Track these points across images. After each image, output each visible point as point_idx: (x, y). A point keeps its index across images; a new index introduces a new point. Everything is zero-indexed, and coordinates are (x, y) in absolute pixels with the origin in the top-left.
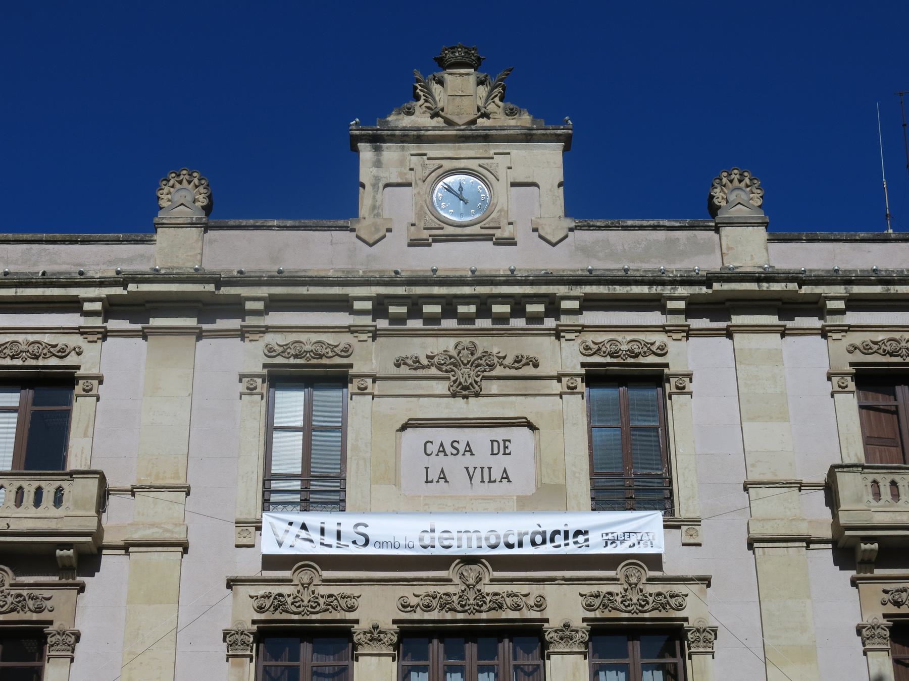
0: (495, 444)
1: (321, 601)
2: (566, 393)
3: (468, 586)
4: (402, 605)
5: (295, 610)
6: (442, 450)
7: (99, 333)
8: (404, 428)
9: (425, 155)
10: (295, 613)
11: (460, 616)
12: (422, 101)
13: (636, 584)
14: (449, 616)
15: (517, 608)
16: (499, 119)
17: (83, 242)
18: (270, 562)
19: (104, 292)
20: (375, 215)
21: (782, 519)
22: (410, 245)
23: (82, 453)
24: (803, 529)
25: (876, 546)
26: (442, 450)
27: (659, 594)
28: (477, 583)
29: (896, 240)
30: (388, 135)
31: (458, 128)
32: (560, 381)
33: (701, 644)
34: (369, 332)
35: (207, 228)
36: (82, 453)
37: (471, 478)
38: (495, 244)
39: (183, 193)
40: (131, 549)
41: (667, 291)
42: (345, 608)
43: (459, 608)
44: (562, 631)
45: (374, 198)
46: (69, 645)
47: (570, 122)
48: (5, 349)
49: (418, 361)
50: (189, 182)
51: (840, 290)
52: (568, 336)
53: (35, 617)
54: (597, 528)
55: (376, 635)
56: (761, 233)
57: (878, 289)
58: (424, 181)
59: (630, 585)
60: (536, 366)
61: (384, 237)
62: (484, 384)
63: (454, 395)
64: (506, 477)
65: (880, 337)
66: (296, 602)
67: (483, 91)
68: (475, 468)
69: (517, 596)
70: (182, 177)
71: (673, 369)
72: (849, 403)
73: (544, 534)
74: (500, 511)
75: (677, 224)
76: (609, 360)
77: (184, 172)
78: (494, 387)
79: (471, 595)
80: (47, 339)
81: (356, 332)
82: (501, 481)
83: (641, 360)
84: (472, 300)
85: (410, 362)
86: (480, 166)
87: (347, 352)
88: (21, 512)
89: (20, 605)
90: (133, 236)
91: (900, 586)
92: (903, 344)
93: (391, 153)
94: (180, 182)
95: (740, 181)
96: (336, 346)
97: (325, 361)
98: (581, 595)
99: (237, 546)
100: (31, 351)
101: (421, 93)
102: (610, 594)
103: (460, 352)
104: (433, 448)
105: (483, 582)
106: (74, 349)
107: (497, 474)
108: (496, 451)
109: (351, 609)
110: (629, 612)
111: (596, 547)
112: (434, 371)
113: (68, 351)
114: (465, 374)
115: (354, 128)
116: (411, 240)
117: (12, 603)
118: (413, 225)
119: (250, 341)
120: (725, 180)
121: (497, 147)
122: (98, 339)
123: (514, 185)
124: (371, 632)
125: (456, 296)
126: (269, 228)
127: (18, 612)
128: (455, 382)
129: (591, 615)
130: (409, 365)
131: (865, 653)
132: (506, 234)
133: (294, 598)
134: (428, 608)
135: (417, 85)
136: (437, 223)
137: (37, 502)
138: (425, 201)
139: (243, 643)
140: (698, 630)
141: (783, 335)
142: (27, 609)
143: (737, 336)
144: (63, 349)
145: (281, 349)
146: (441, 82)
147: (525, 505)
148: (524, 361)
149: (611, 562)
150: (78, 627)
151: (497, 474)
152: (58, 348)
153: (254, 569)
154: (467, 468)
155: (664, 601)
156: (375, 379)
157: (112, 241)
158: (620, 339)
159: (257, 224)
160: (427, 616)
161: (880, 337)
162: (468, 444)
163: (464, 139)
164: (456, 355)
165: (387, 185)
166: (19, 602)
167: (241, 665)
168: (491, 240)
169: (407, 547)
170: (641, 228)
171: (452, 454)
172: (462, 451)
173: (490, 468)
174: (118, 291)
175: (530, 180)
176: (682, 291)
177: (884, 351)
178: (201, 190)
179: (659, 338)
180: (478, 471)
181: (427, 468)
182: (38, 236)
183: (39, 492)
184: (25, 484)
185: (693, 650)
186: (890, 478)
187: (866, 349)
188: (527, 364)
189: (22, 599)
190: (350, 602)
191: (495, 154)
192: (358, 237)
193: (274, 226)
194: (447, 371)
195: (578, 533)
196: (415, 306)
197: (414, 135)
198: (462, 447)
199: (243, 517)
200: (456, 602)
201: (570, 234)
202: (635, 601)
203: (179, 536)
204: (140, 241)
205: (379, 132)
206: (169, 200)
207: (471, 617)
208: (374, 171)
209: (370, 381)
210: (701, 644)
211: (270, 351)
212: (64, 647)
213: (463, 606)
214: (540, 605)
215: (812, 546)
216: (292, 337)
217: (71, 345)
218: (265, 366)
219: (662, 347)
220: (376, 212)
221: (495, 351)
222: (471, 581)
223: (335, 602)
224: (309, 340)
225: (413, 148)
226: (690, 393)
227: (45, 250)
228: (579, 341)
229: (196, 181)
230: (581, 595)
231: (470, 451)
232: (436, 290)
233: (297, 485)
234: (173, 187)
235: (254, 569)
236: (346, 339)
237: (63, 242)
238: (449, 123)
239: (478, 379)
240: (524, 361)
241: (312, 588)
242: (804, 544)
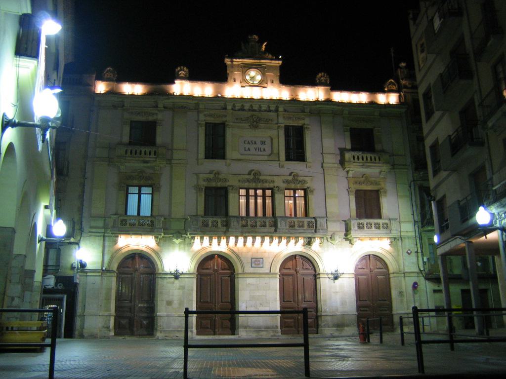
64: (264, 149)
104: (246, 142)
107: (262, 150)
184: (147, 150)
198: (253, 142)
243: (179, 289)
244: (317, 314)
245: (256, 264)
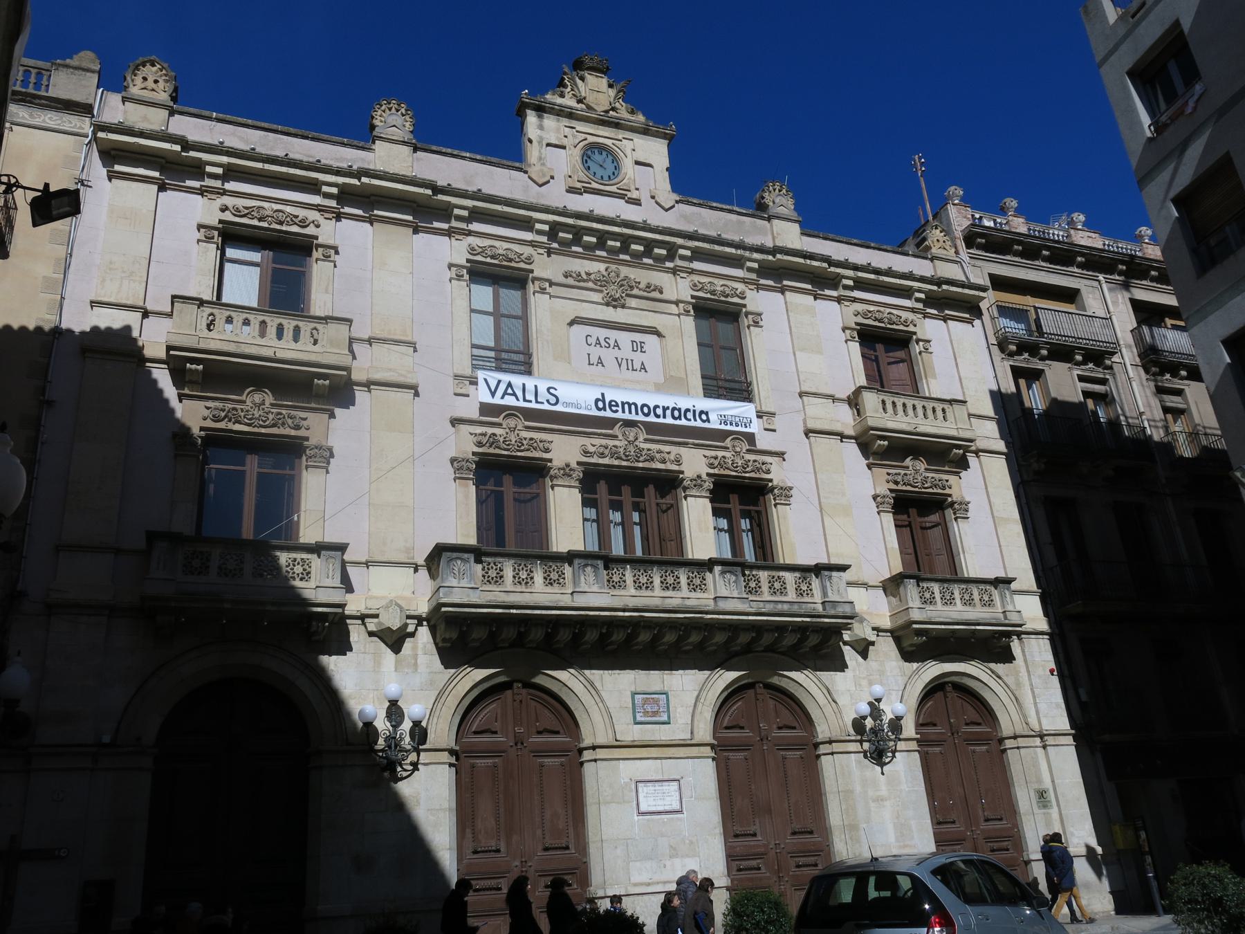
0: (635, 344)
1: (525, 442)
2: (683, 314)
3: (629, 442)
4: (583, 450)
5: (506, 447)
6: (598, 343)
7: (334, 212)
8: (571, 323)
9: (574, 128)
10: (505, 450)
11: (624, 463)
12: (569, 89)
13: (740, 452)
14: (616, 463)
15: (664, 462)
16: (623, 113)
17: (313, 139)
18: (486, 409)
19: (341, 180)
20: (541, 164)
21: (826, 419)
22: (568, 191)
23: (325, 305)
24: (837, 427)
25: (886, 443)
26: (598, 343)
27: (755, 461)
28: (635, 440)
29: (874, 248)
30: (549, 108)
31: (599, 113)
32: (677, 306)
33: (783, 498)
34: (545, 248)
35: (416, 149)
36: (325, 305)
37: (620, 366)
38: (627, 202)
39: (394, 117)
40: (372, 387)
41: (747, 254)
42: (543, 449)
43: (624, 458)
44: (695, 480)
45: (540, 151)
46: (325, 458)
47: (673, 126)
48: (252, 211)
49: (580, 276)
50: (398, 111)
51: (850, 273)
52: (682, 275)
53: (293, 433)
54: (714, 410)
55: (567, 470)
56: (796, 228)
57: (872, 276)
58: (575, 147)
59: (736, 452)
60: (661, 292)
61: (548, 182)
62: (628, 299)
63: (607, 304)
64: (643, 368)
65: (872, 308)
66: (506, 441)
67: (612, 92)
68: (622, 359)
69: (663, 452)
70: (392, 105)
71: (750, 308)
72: (855, 347)
73: (679, 410)
74: (646, 391)
75: (744, 212)
76: (709, 296)
77: (394, 102)
78: (633, 302)
79: (632, 449)
80: (289, 209)
81: (536, 246)
82: (640, 371)
83: (730, 299)
84: (619, 238)
85: (574, 275)
86: (613, 144)
87: (529, 260)
88: (282, 344)
89: (280, 422)
90: (355, 142)
91: (897, 471)
92: (886, 315)
93: (550, 121)
94: (390, 109)
95: (780, 191)
96: (522, 255)
97: (513, 264)
98: (705, 457)
99: (456, 394)
100: (275, 217)
101: (569, 84)
102: (724, 457)
103: (609, 274)
104: (592, 340)
105: (638, 440)
106: (313, 222)
107: (637, 365)
108: (635, 349)
109: (547, 451)
110: (736, 471)
111: (715, 424)
112: (590, 285)
113: (308, 223)
114: (613, 290)
115: (525, 96)
116: (569, 187)
117: (273, 419)
118: (570, 177)
119: (457, 239)
120: (771, 188)
121: (624, 134)
122: (333, 217)
123: (637, 163)
124: (563, 469)
125: (608, 232)
126: (463, 158)
127: (279, 428)
128: (608, 294)
129: (712, 471)
130: (573, 277)
131: (878, 513)
132: (634, 197)
133: (505, 438)
134: (602, 455)
135: (565, 77)
136: (586, 179)
137: (296, 338)
138: (577, 161)
139: (468, 469)
140: (782, 488)
141: (815, 299)
142: (287, 426)
143: (787, 293)
144: (304, 220)
145: (480, 250)
146: (582, 79)
147: (659, 389)
148: (652, 288)
149: (723, 435)
150: (330, 444)
151: (637, 365)
152: (299, 219)
153: (474, 414)
154: (617, 358)
155: (758, 466)
156: (551, 284)
157: (338, 143)
158: (716, 282)
159: (454, 153)
160: (601, 461)
161: (872, 308)
162: (616, 341)
163: (601, 122)
164: (607, 275)
165: (548, 145)
166: (280, 419)
167: (467, 486)
168: (624, 198)
169: (586, 408)
170: (722, 210)
171: (605, 347)
172: (612, 346)
173: (632, 360)
174: (354, 181)
175: (647, 162)
176: (756, 256)
177: (875, 317)
178: (408, 119)
179: (740, 287)
180: (624, 361)
181: (589, 355)
182: (275, 127)
183: (297, 330)
184: (285, 322)
185: (777, 501)
186: (892, 399)
187: (865, 316)
188: (654, 290)
189: (282, 416)
190: (547, 445)
191: (624, 138)
192: (529, 177)
193: (466, 157)
194: (601, 286)
195: (702, 412)
196: (578, 233)
197: (568, 112)
198: (612, 342)
199: (460, 372)
200: (622, 453)
201: (676, 205)
202: (740, 464)
203: (410, 380)
204: (361, 147)
205: (543, 104)
206: (381, 121)
207: (632, 465)
208: (539, 132)
209: (547, 284)
210: (783, 498)
211: (472, 250)
212: (320, 459)
213: (627, 456)
214: (678, 461)
215: (844, 440)
216: (487, 242)
217: (311, 219)
218: (468, 261)
219: (743, 293)
220: (542, 162)
221: (633, 277)
222: (631, 438)
223: (535, 444)
224: (501, 246)
225: (566, 122)
226: (761, 327)
227: (280, 139)
228: (689, 279)
229: (403, 111)
230: (705, 457)
231: (618, 346)
232: (595, 225)
233: (492, 354)
234: (384, 111)
235: (474, 414)
236: (527, 251)
237: (296, 136)
238: (589, 108)
239: (624, 295)
240: (652, 288)
241: (516, 432)
242: (839, 438)
245: (646, 713)
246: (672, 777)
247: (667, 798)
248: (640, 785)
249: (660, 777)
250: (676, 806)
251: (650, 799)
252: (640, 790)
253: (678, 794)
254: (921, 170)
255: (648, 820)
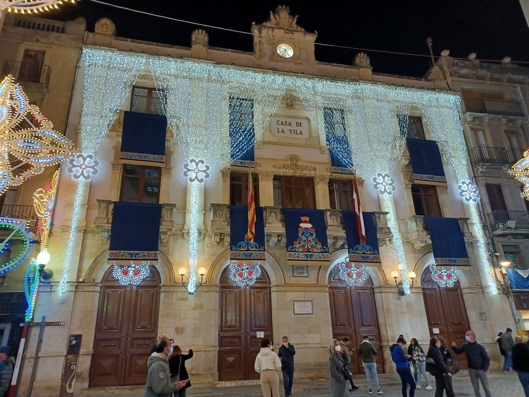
63: (287, 108)
64: (301, 132)
107: (298, 132)
151: (298, 132)
180: (293, 131)
198: (288, 123)
208: (260, 39)
222: (294, 162)
229: (204, 34)
243: (195, 309)
244: (380, 344)
246: (309, 300)
247: (307, 308)
248: (295, 302)
249: (304, 300)
250: (310, 312)
251: (299, 308)
252: (295, 304)
253: (311, 307)
254: (430, 45)
255: (298, 317)
